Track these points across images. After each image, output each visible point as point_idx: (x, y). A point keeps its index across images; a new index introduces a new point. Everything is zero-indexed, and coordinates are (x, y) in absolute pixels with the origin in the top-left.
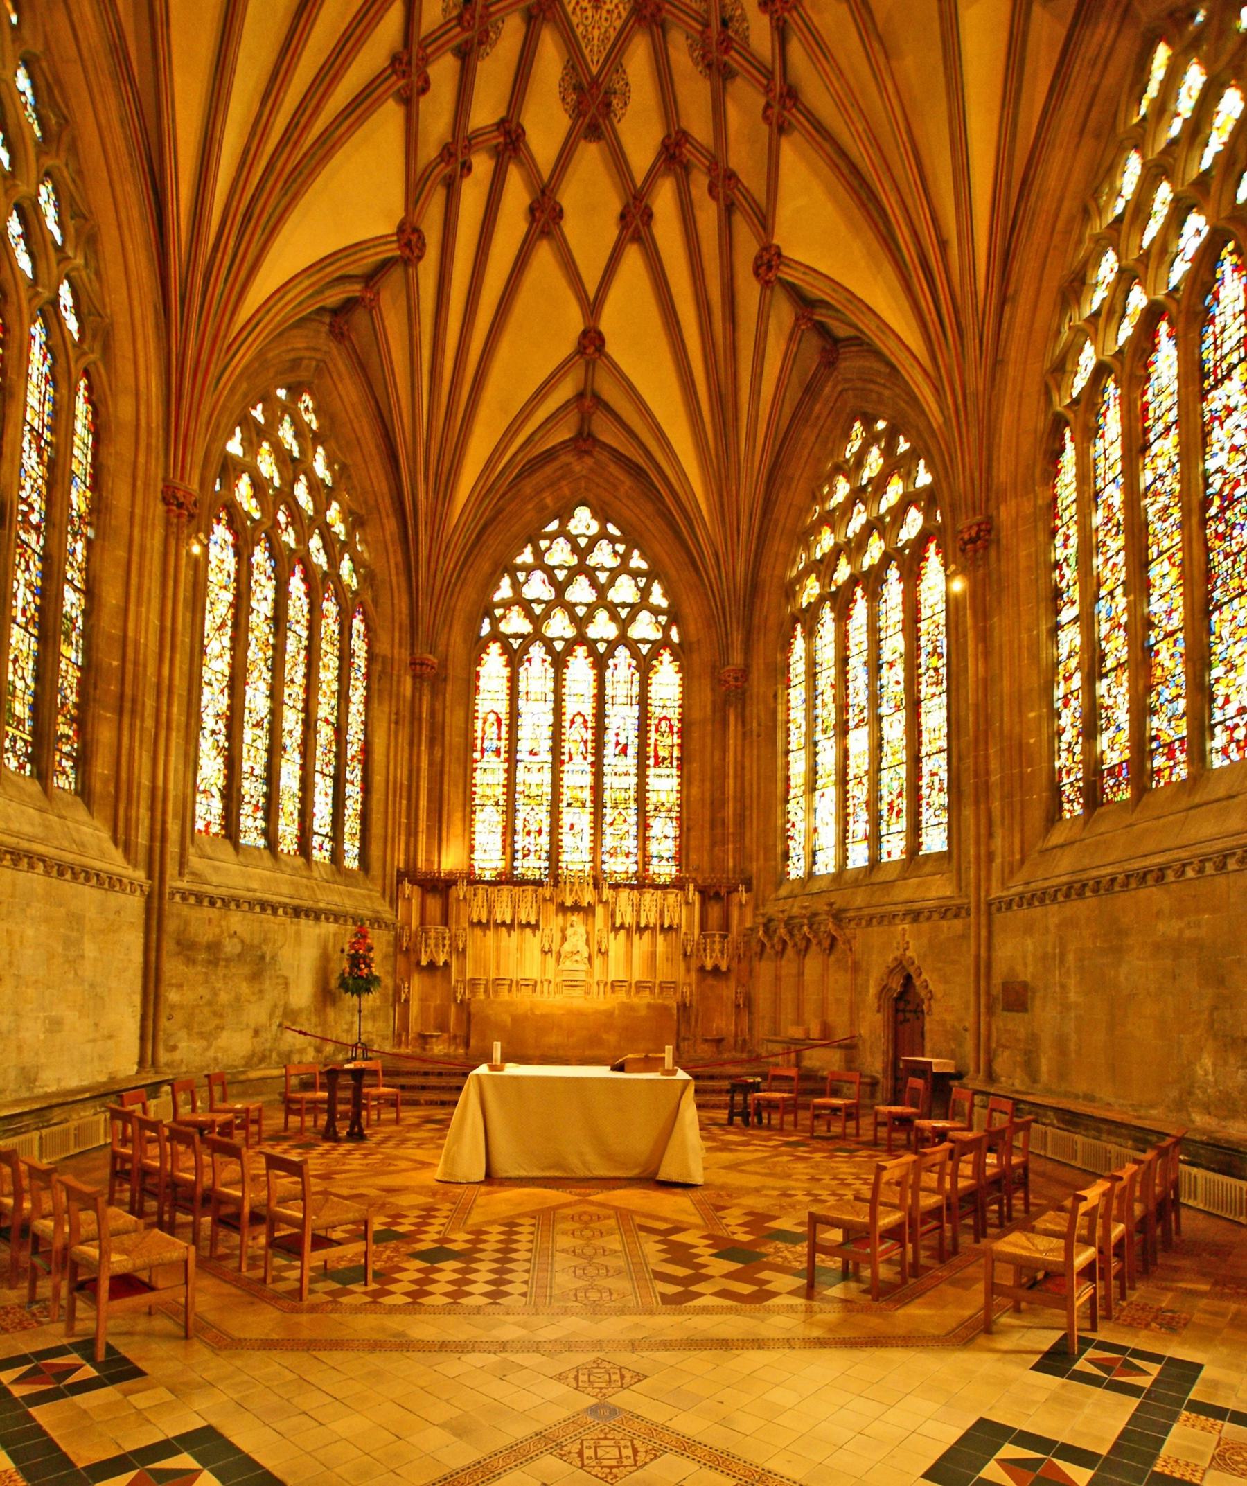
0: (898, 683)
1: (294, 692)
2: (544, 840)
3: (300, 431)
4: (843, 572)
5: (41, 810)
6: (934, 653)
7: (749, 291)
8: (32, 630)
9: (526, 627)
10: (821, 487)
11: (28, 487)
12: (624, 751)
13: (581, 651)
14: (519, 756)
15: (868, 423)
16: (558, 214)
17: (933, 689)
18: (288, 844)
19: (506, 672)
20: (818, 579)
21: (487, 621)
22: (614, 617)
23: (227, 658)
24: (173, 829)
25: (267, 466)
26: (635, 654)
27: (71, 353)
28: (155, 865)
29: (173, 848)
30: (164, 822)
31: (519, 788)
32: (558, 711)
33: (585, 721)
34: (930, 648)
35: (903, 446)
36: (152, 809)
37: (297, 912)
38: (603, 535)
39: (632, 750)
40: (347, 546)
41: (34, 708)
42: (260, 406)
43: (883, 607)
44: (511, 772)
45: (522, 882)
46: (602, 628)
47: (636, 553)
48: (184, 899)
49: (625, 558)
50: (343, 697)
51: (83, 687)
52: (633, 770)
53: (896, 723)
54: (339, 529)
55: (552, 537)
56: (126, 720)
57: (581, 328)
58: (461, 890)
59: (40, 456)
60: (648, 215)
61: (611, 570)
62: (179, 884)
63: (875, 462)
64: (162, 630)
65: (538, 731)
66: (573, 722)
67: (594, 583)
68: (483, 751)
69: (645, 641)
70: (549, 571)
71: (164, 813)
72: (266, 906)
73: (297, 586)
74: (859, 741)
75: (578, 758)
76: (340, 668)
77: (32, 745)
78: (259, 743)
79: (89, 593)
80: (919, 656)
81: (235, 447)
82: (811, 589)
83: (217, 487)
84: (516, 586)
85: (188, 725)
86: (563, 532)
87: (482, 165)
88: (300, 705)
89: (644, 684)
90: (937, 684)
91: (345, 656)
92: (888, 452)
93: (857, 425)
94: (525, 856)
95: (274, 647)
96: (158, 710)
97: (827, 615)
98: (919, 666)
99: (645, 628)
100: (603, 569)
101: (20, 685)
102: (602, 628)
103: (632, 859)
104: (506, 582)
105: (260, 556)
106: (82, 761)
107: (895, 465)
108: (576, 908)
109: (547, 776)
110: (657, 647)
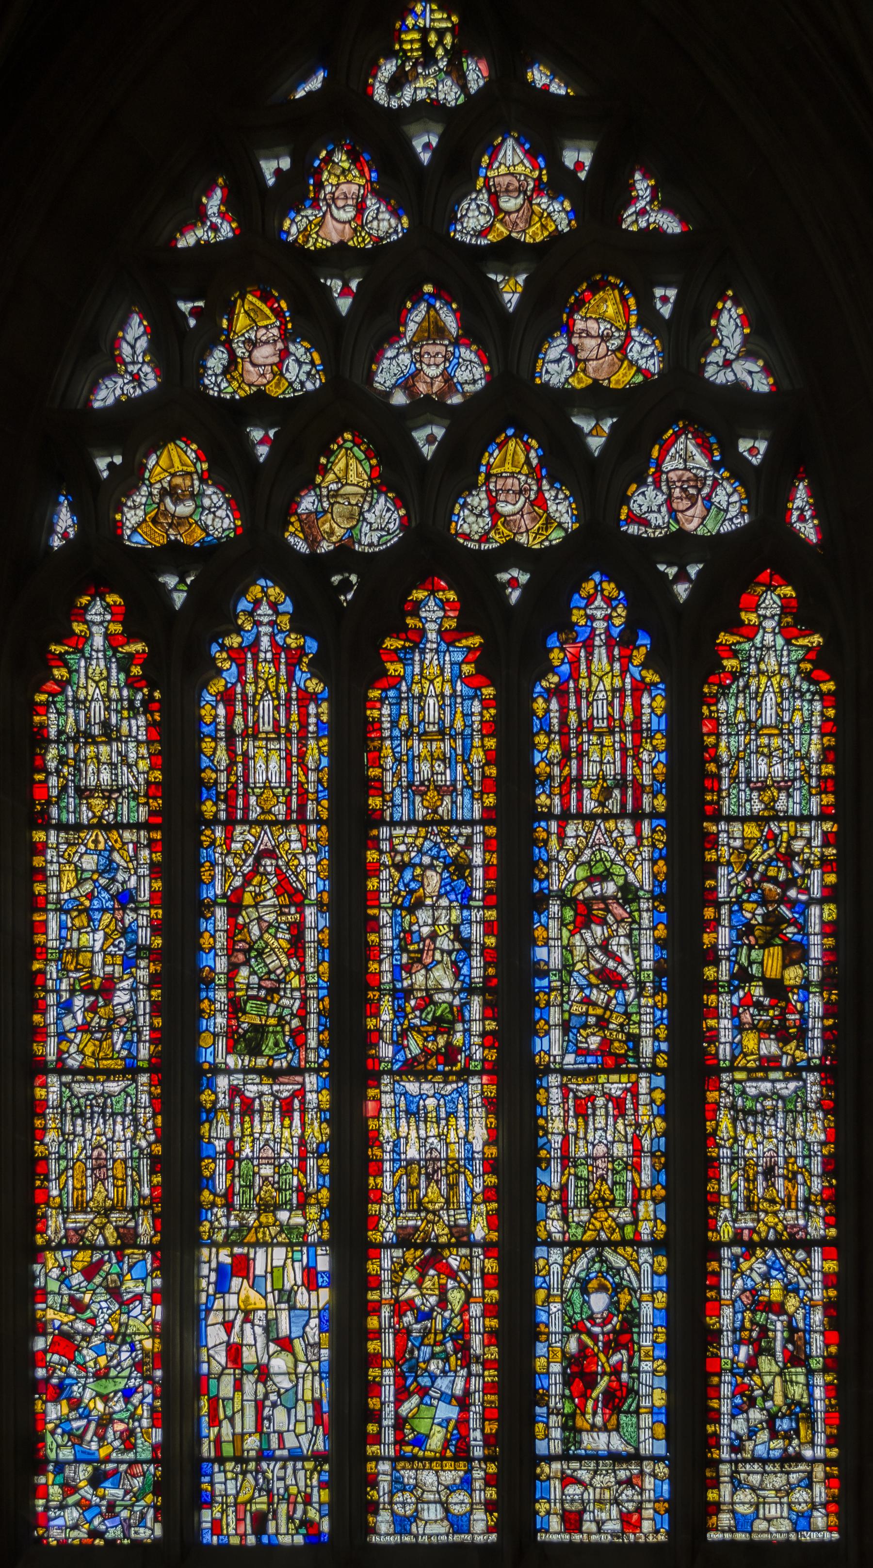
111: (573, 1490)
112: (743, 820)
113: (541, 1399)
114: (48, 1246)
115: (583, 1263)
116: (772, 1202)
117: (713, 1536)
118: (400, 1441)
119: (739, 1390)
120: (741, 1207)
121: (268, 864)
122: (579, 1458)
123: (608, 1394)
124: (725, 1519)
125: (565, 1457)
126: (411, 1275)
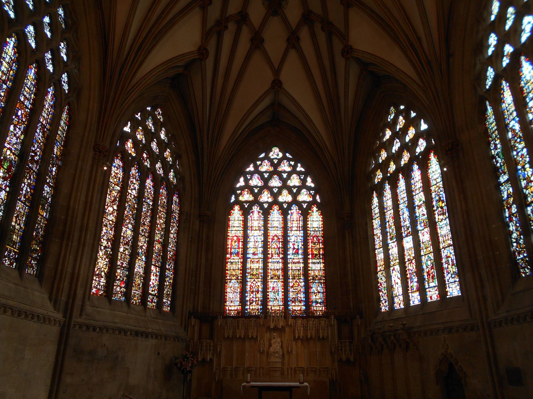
0: (424, 215)
1: (144, 229)
2: (260, 295)
3: (156, 122)
4: (392, 167)
5: (16, 284)
6: (439, 200)
7: (340, 62)
8: (27, 204)
9: (251, 198)
10: (379, 134)
11: (36, 146)
12: (297, 253)
13: (276, 208)
14: (248, 256)
15: (397, 107)
16: (262, 41)
17: (441, 217)
18: (136, 300)
19: (241, 218)
20: (381, 171)
21: (233, 196)
22: (290, 192)
23: (115, 214)
24: (80, 292)
25: (140, 136)
26: (300, 207)
27: (64, 97)
28: (68, 311)
29: (78, 302)
30: (76, 290)
31: (248, 271)
32: (266, 235)
33: (279, 239)
34: (437, 198)
35: (413, 114)
36: (71, 283)
37: (137, 334)
38: (284, 158)
39: (300, 252)
40: (173, 166)
41: (22, 238)
42: (139, 114)
43: (412, 181)
44: (244, 263)
45: (250, 316)
46: (285, 197)
47: (299, 165)
48: (80, 328)
49: (295, 167)
50: (167, 231)
51: (48, 228)
52: (301, 261)
53: (425, 233)
54: (170, 159)
55: (262, 160)
56: (65, 242)
57: (273, 79)
58: (220, 321)
59: (43, 134)
60: (298, 39)
61: (288, 172)
62: (79, 320)
63: (401, 121)
64: (86, 202)
65: (257, 244)
66: (273, 239)
67: (281, 178)
68: (231, 254)
69: (304, 202)
70: (261, 174)
71: (76, 285)
72: (122, 331)
73: (149, 183)
74: (408, 243)
75: (275, 256)
76: (166, 218)
77: (18, 254)
78: (127, 252)
79: (56, 188)
80: (432, 202)
81: (127, 129)
82: (379, 175)
83: (118, 144)
84: (246, 181)
85: (93, 244)
86: (267, 157)
87: (232, 27)
88: (147, 234)
89: (305, 221)
90: (443, 214)
91: (169, 213)
92: (407, 117)
93: (392, 108)
94: (250, 303)
95: (137, 209)
96: (80, 237)
97: (387, 187)
98: (433, 207)
99: (304, 197)
100: (285, 172)
101: (17, 227)
102: (285, 197)
103: (302, 304)
104: (242, 179)
105: (133, 171)
106: (41, 262)
107: (410, 123)
108: (276, 329)
109: (261, 265)
110: (310, 205)
111: (430, 292)
112: (434, 185)
113: (424, 279)
114: (378, 272)
115: (426, 257)
116: (446, 240)
117: (448, 297)
118: (411, 290)
119: (447, 272)
120: (443, 242)
121: (391, 215)
122: (430, 288)
123: (432, 276)
124: (449, 294)
125: (429, 288)
126: (410, 265)
